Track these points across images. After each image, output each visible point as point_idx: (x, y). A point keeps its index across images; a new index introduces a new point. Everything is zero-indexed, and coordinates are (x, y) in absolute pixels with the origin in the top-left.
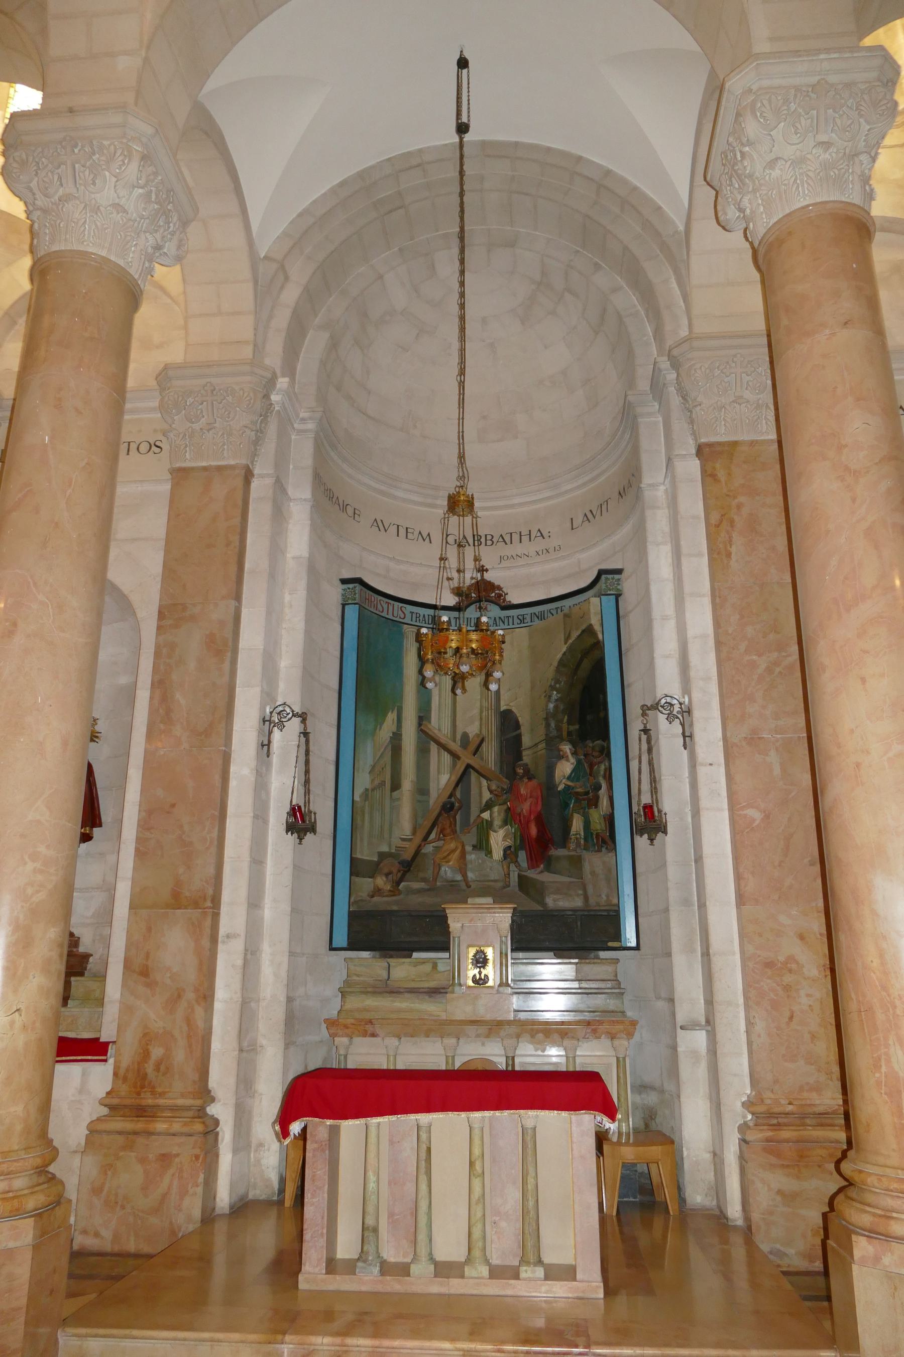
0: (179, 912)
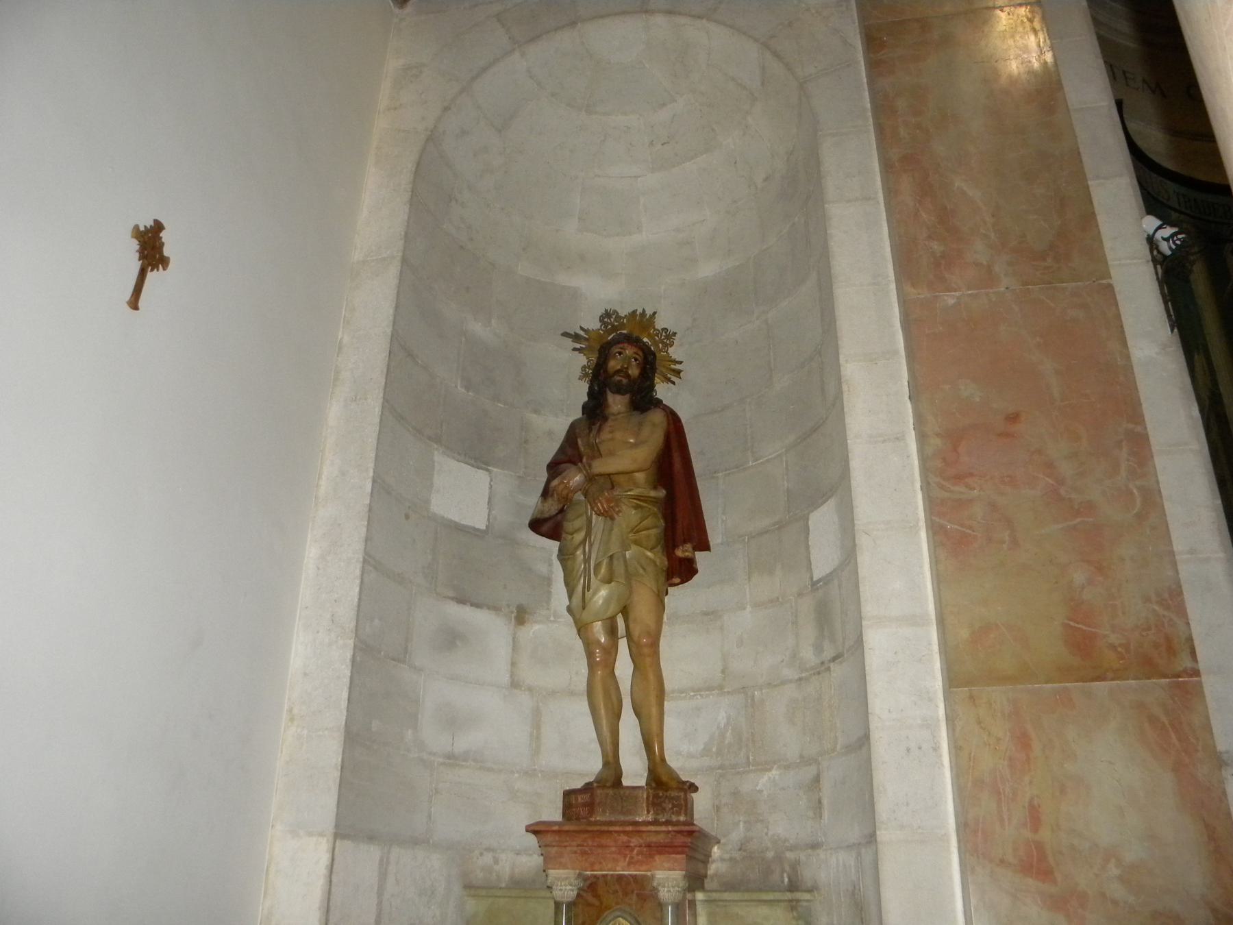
0: (1101, 688)
